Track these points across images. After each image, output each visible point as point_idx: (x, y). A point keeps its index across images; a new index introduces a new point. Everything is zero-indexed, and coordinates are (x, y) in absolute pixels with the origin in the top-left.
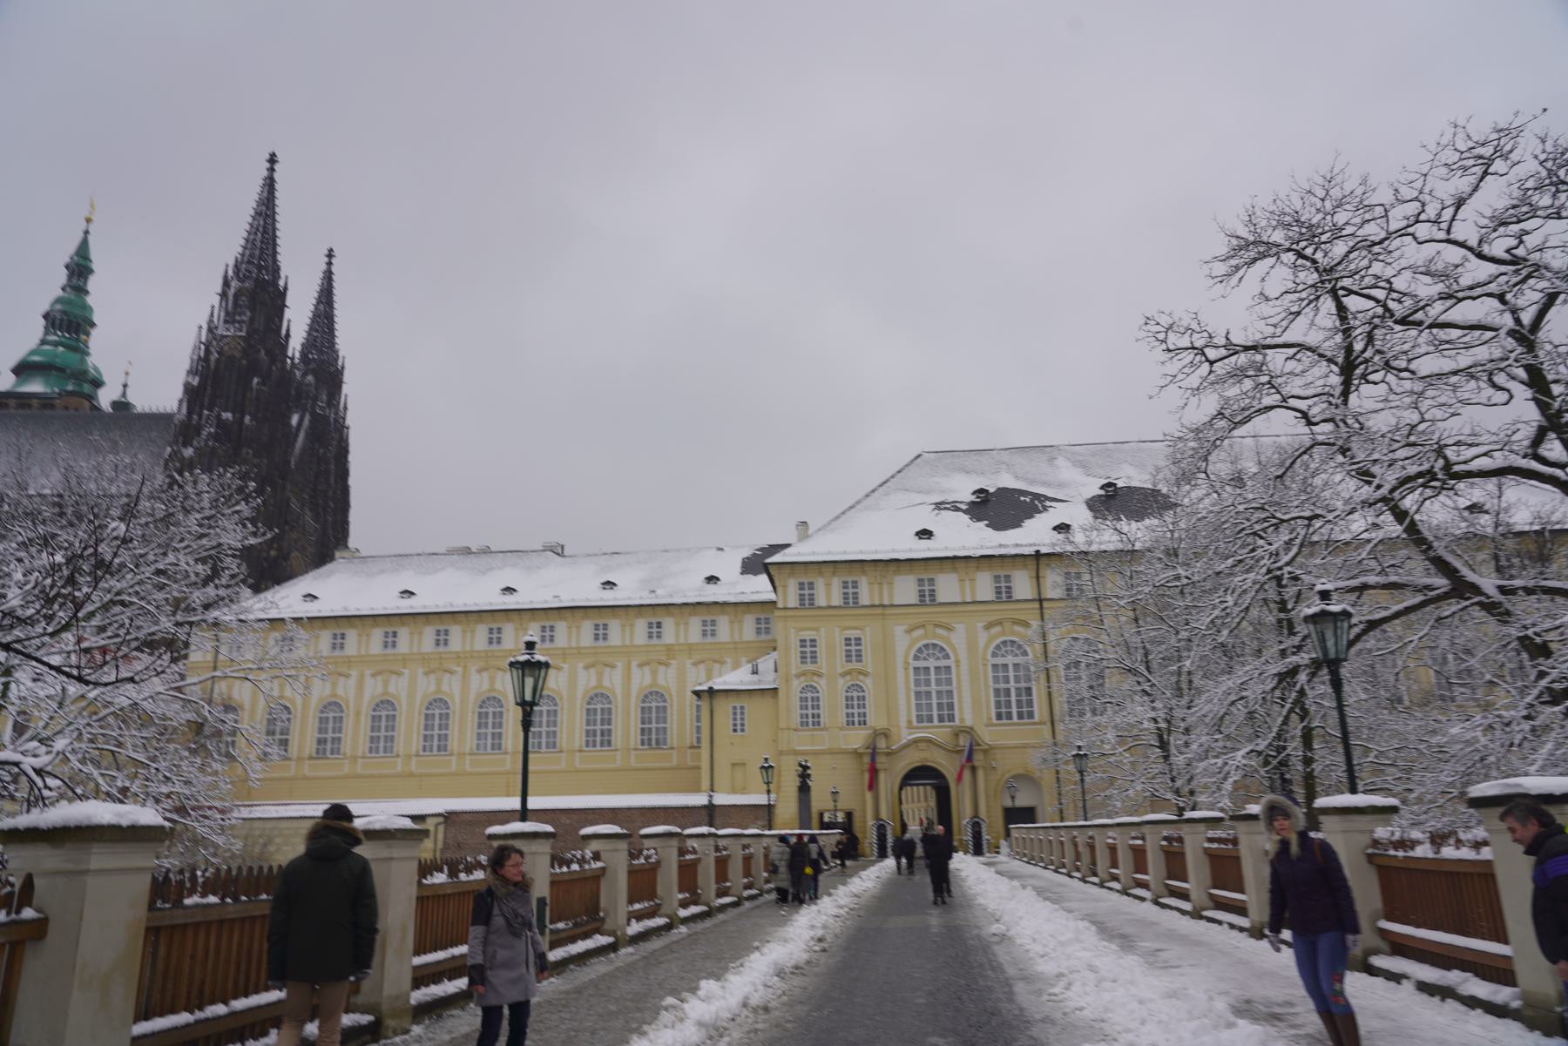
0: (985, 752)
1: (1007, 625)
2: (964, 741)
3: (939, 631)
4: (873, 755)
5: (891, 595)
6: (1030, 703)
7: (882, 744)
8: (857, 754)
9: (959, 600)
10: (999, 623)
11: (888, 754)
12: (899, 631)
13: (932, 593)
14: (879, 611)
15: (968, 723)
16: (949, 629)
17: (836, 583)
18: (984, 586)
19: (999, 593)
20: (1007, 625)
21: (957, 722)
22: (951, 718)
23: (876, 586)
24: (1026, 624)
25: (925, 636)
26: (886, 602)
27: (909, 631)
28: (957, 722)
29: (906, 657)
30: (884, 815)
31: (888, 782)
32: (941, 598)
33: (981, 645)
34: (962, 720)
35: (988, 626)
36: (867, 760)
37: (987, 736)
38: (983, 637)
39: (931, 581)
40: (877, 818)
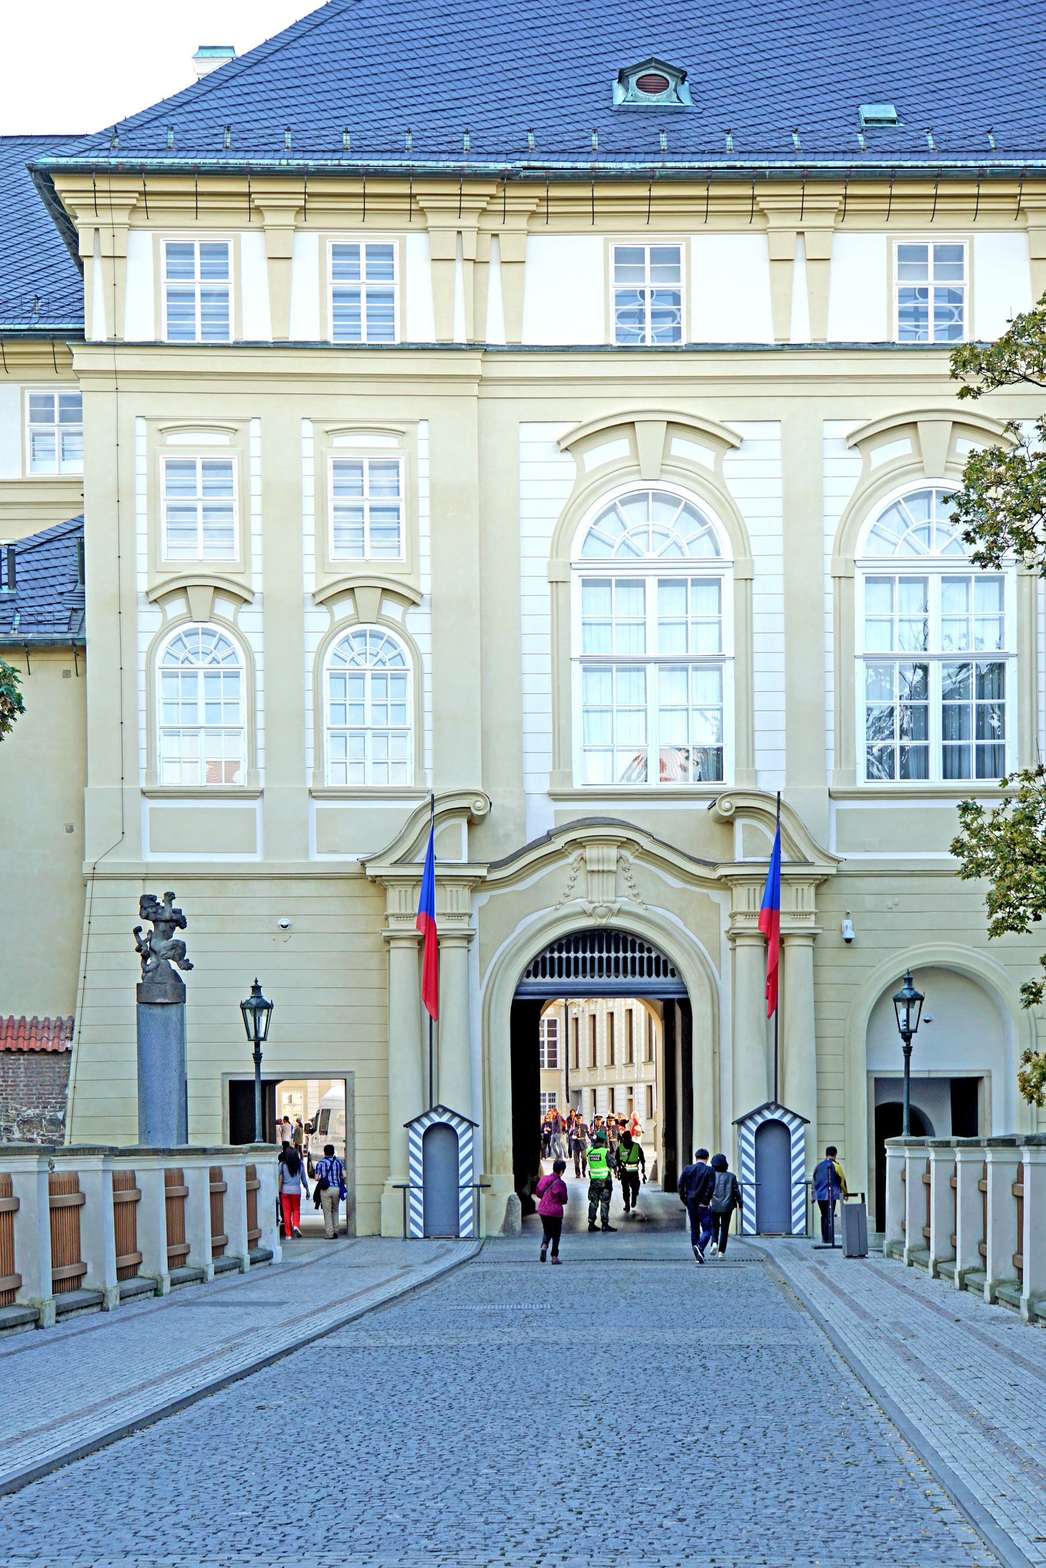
0: (822, 882)
2: (749, 845)
3: (684, 447)
4: (429, 883)
5: (514, 313)
7: (455, 848)
12: (537, 444)
14: (473, 364)
15: (771, 782)
21: (730, 781)
26: (495, 336)
28: (730, 781)
32: (698, 329)
36: (404, 902)
37: (830, 836)
38: (843, 473)
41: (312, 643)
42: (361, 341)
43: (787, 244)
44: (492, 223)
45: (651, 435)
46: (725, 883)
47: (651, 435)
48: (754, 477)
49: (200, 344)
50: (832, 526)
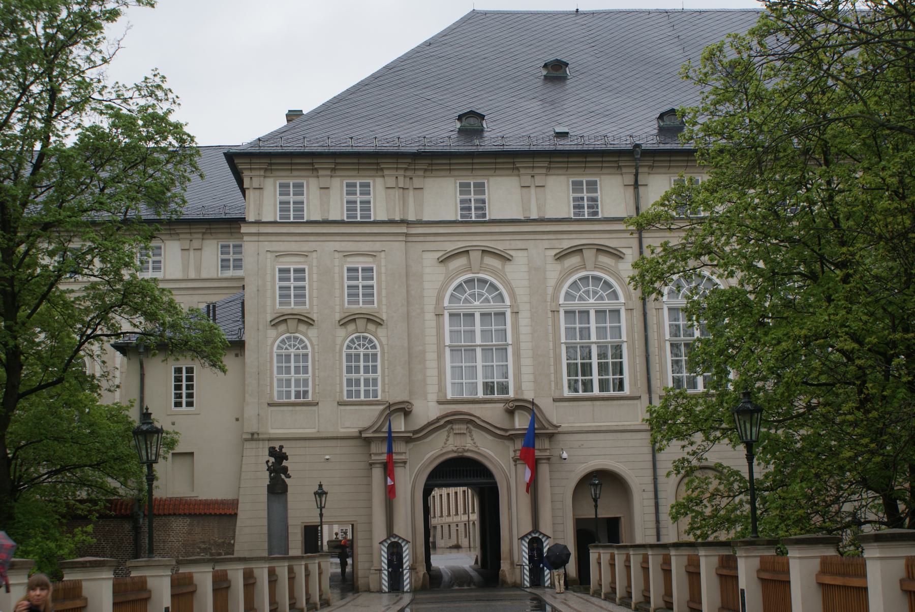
0: (551, 436)
1: (589, 254)
2: (521, 422)
3: (490, 261)
6: (619, 368)
8: (364, 440)
9: (521, 217)
10: (577, 251)
11: (408, 440)
13: (481, 208)
14: (404, 230)
15: (529, 395)
16: (505, 258)
17: (338, 186)
18: (556, 195)
19: (578, 207)
20: (589, 254)
21: (511, 394)
22: (504, 389)
23: (397, 193)
24: (618, 255)
25: (469, 269)
26: (411, 217)
27: (443, 261)
29: (439, 298)
30: (402, 528)
31: (408, 482)
32: (493, 213)
33: (552, 282)
34: (518, 388)
35: (561, 256)
38: (554, 271)
39: (480, 188)
40: (390, 532)
41: (339, 341)
42: (357, 223)
43: (527, 180)
44: (409, 173)
45: (475, 256)
46: (511, 438)
47: (475, 256)
48: (517, 273)
49: (293, 223)
50: (550, 291)
